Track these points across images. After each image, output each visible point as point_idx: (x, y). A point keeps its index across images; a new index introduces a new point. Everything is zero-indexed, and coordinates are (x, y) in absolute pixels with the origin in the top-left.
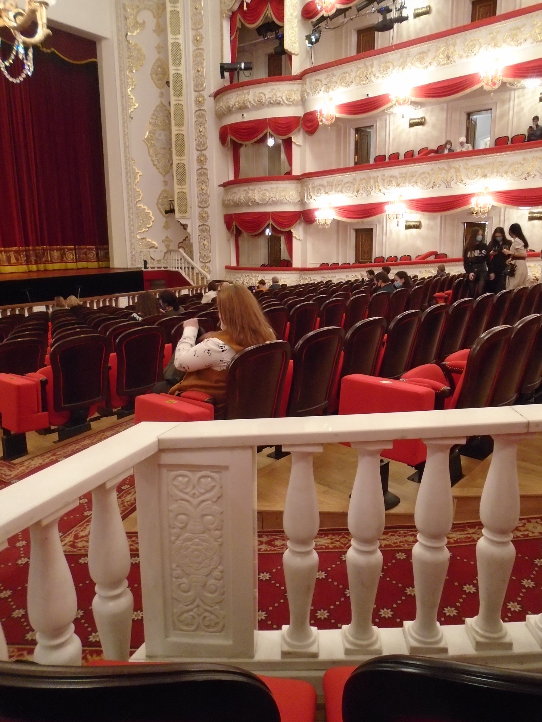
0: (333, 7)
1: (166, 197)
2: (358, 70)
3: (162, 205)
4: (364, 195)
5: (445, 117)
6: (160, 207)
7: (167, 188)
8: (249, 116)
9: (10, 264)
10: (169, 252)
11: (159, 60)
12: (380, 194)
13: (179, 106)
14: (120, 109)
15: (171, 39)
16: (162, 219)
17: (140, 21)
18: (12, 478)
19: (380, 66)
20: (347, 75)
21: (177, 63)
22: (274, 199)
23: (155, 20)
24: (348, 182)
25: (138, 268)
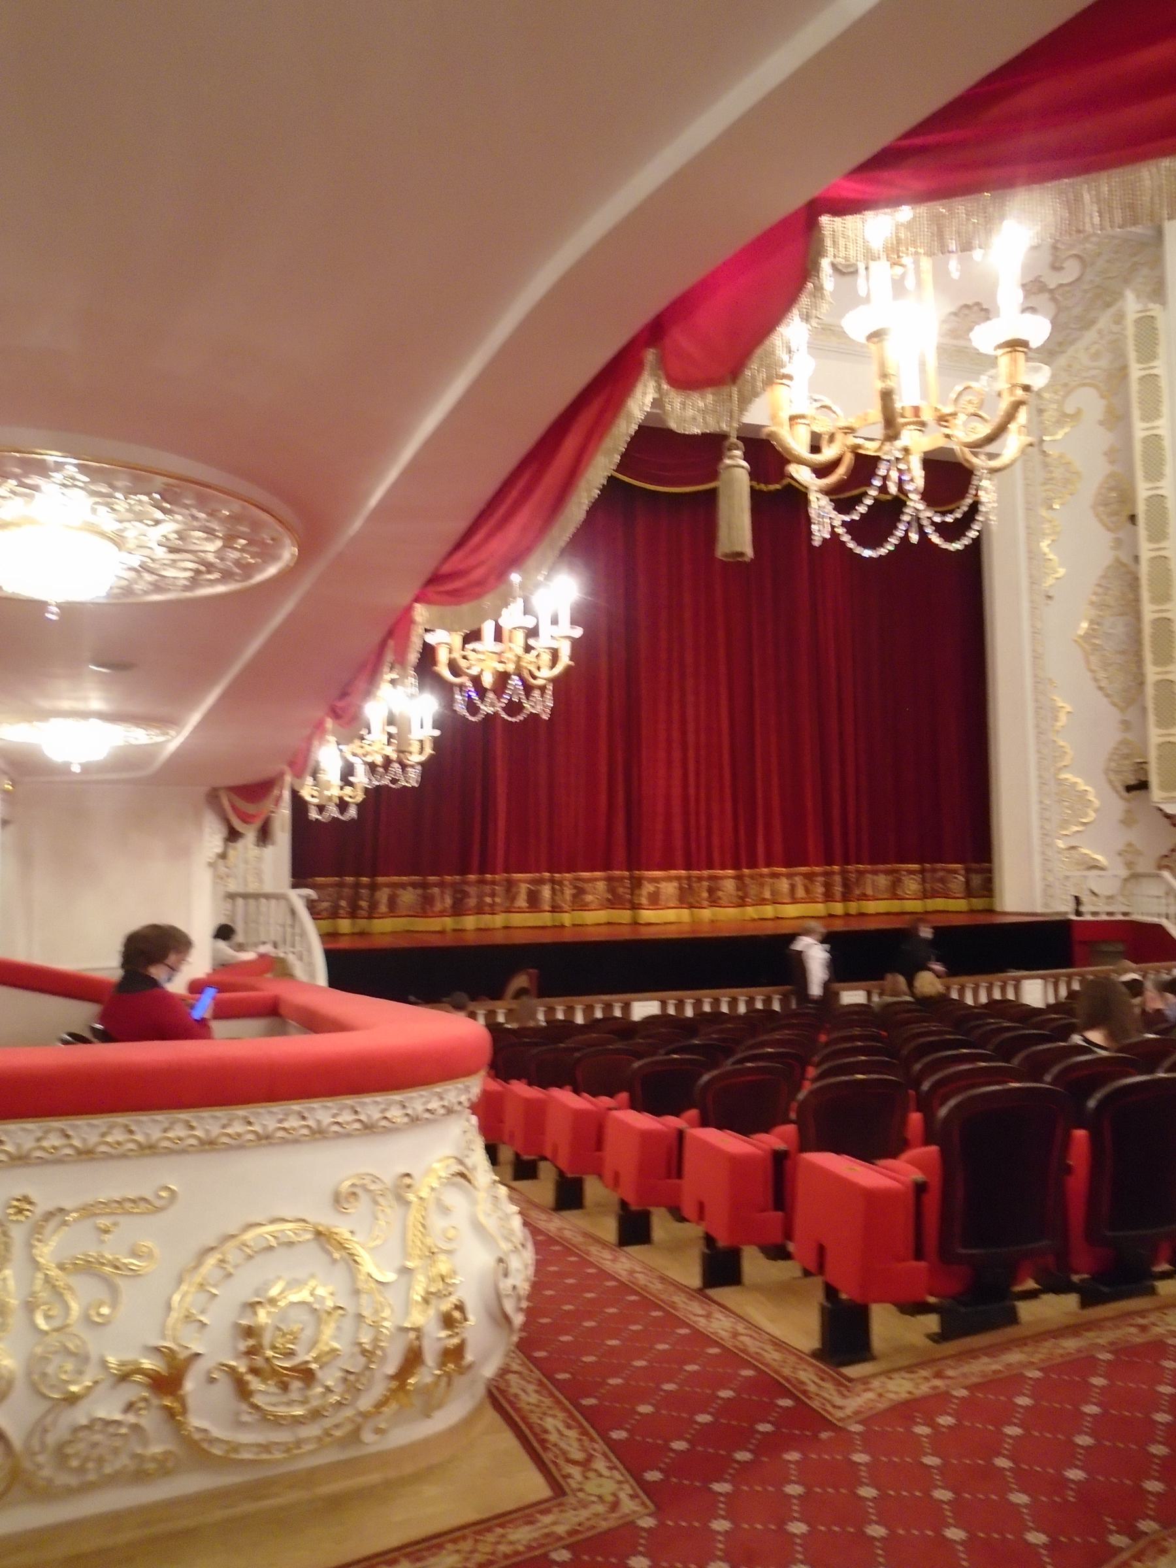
1: (1127, 757)
3: (1117, 772)
6: (1113, 777)
7: (1129, 736)
9: (794, 901)
10: (1135, 876)
11: (1111, 475)
14: (1024, 583)
15: (1140, 430)
16: (1117, 804)
17: (1070, 409)
18: (849, 1417)
21: (1155, 472)
23: (1103, 402)
25: (1058, 914)
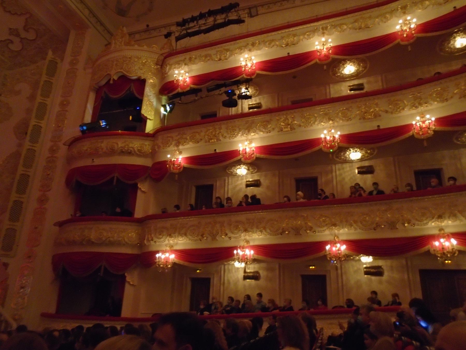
0: (188, 86)
2: (207, 131)
4: (210, 238)
8: (98, 162)
12: (227, 239)
13: (31, 152)
19: (227, 128)
20: (197, 134)
22: (111, 239)
24: (193, 226)
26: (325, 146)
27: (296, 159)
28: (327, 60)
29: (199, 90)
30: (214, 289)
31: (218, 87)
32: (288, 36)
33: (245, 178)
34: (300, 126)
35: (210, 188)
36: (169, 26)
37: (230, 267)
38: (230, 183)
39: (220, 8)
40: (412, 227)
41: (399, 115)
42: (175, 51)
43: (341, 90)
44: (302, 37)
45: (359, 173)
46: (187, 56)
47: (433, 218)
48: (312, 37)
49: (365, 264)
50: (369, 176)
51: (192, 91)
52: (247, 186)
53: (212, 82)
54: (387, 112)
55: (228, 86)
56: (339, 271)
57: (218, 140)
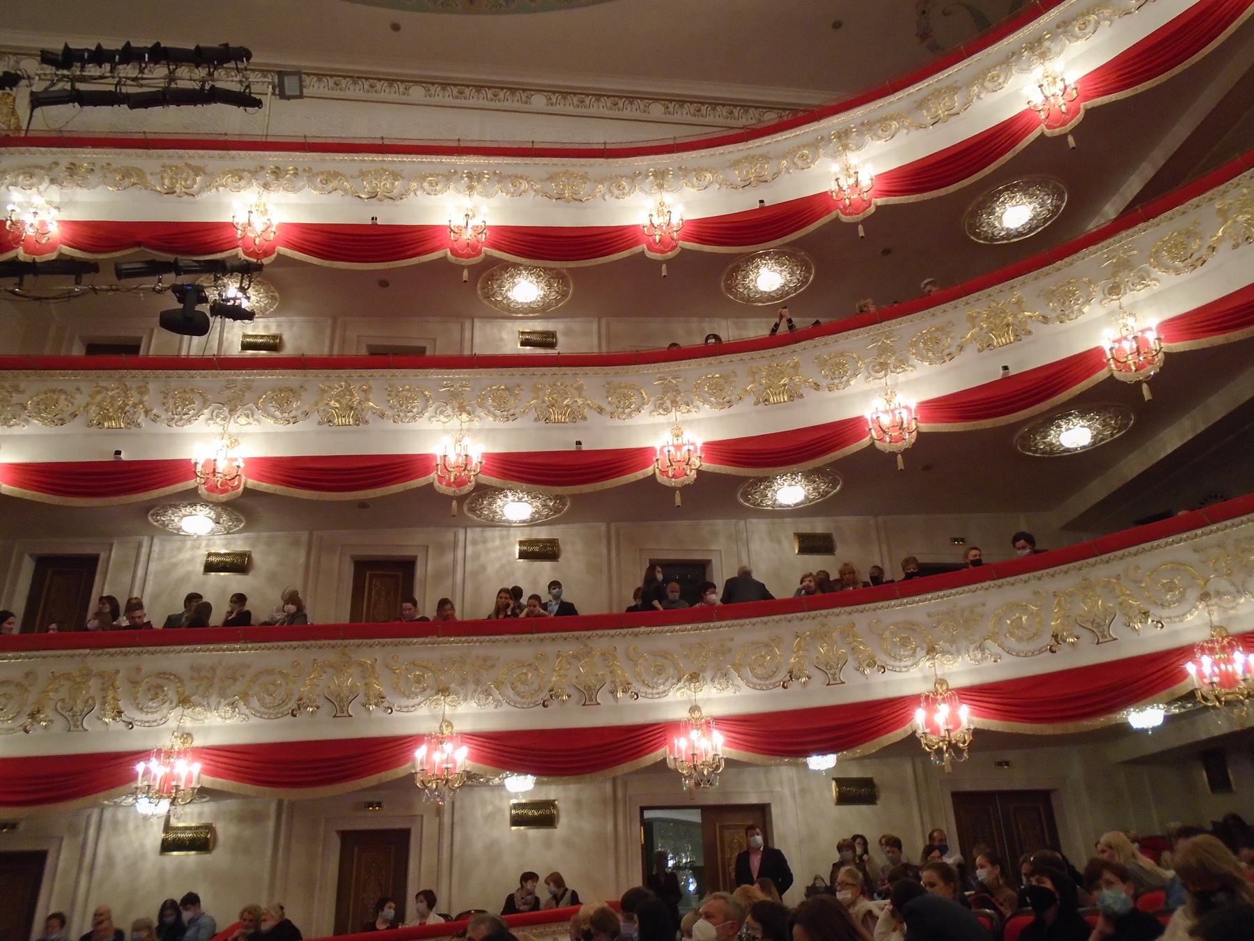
0: (52, 247)
2: (99, 392)
4: (59, 724)
5: (302, 560)
20: (63, 397)
26: (441, 478)
27: (363, 505)
28: (473, 256)
29: (92, 267)
30: (57, 886)
31: (155, 268)
32: (378, 174)
33: (204, 543)
34: (382, 416)
35: (86, 567)
36: (15, 54)
37: (121, 815)
38: (154, 555)
39: (191, 47)
40: (632, 702)
41: (628, 422)
42: (23, 134)
43: (502, 339)
44: (414, 185)
45: (523, 555)
46: (64, 156)
47: (679, 681)
48: (441, 192)
49: (516, 795)
50: (547, 565)
51: (64, 266)
52: (210, 568)
53: (137, 249)
54: (601, 410)
55: (187, 272)
56: (447, 818)
57: (133, 423)
